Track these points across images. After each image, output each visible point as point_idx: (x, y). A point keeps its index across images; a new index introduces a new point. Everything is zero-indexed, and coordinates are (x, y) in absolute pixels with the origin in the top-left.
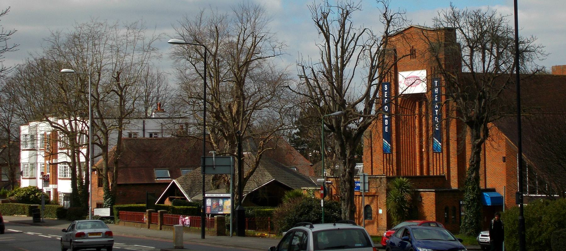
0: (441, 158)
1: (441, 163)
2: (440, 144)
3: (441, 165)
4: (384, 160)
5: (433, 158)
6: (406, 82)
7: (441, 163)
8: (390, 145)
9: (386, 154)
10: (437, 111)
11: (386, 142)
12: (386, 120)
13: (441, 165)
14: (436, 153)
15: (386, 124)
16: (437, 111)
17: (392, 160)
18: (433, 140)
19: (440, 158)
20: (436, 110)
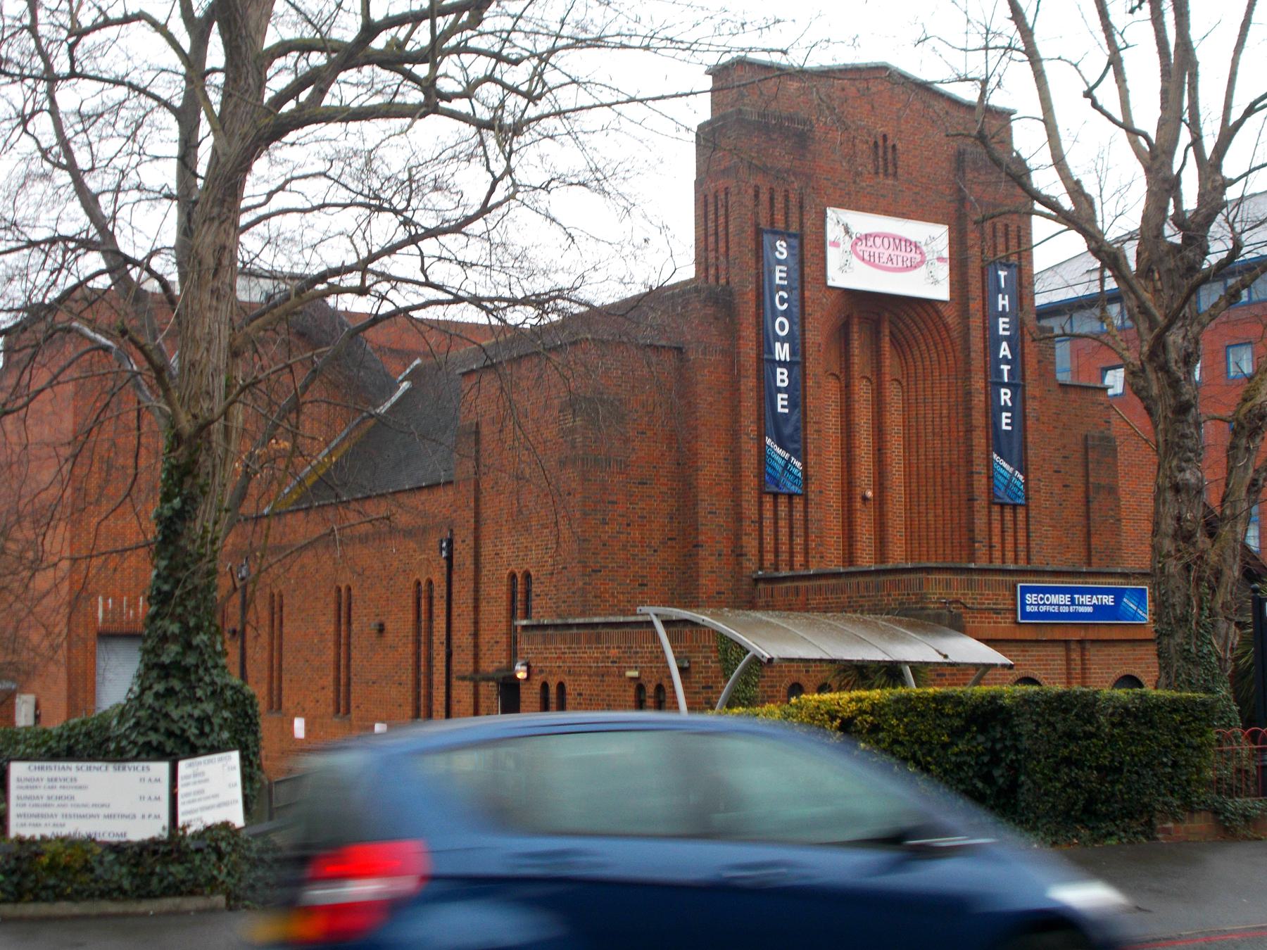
0: (1021, 524)
1: (1022, 538)
2: (1021, 477)
3: (1021, 547)
5: (990, 523)
6: (858, 248)
7: (1022, 538)
8: (798, 464)
9: (775, 496)
10: (1005, 368)
11: (779, 451)
12: (779, 370)
13: (1021, 547)
14: (1002, 506)
15: (779, 384)
16: (1005, 368)
17: (806, 520)
18: (990, 462)
19: (1015, 524)
20: (1002, 367)
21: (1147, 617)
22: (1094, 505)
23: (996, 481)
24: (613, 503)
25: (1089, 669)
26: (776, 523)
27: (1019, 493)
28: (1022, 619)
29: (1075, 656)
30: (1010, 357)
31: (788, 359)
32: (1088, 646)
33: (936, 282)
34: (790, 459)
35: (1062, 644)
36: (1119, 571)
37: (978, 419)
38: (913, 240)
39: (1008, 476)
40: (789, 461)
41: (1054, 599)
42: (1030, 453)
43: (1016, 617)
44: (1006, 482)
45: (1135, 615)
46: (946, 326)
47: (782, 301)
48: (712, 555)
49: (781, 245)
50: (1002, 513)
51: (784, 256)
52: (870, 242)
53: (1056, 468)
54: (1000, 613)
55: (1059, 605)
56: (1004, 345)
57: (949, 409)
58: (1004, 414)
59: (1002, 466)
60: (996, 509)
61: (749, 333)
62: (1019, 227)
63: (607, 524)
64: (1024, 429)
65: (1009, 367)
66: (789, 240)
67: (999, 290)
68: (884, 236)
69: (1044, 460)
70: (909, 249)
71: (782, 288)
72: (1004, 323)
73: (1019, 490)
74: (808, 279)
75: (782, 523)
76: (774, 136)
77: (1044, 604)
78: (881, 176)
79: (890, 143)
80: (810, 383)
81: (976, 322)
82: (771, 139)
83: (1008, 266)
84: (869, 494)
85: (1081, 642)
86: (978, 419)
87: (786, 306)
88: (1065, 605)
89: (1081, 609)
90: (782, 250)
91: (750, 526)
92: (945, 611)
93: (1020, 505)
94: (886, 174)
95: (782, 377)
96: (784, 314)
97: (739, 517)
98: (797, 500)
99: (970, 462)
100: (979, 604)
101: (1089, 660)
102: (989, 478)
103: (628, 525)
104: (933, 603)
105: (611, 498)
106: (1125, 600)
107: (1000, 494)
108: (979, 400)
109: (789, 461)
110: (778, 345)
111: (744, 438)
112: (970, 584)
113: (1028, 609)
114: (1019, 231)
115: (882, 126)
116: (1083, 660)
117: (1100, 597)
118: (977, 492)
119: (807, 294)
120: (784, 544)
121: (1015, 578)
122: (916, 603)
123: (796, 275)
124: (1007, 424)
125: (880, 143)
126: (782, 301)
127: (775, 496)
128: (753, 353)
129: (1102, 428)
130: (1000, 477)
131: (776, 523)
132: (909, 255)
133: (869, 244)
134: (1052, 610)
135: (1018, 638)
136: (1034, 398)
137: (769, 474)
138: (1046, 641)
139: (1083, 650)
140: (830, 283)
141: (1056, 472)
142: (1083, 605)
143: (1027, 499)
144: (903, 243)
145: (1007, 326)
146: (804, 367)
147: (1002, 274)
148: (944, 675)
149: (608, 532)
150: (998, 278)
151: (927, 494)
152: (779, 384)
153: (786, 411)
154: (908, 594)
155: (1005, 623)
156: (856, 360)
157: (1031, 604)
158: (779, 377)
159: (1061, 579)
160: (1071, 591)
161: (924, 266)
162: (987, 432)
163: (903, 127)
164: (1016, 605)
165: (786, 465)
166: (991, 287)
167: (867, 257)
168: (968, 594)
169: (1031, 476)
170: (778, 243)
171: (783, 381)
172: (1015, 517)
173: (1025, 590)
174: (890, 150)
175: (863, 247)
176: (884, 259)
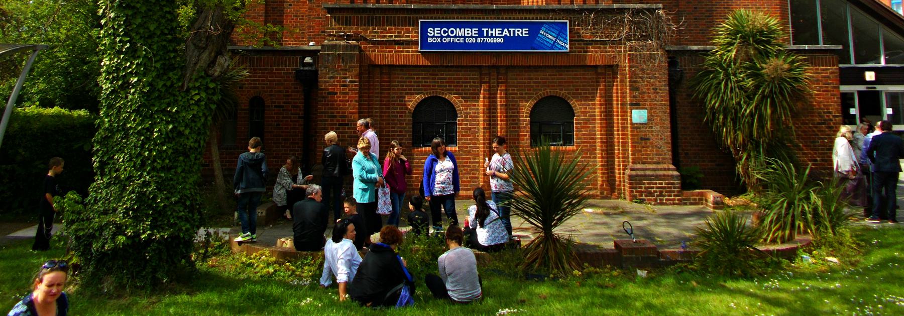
21: (568, 46)
41: (459, 32)
55: (465, 37)
77: (448, 36)
88: (472, 37)
89: (491, 40)
106: (541, 32)
113: (430, 40)
117: (512, 30)
134: (456, 40)
138: (451, 67)
142: (492, 36)
157: (432, 37)
160: (479, 26)
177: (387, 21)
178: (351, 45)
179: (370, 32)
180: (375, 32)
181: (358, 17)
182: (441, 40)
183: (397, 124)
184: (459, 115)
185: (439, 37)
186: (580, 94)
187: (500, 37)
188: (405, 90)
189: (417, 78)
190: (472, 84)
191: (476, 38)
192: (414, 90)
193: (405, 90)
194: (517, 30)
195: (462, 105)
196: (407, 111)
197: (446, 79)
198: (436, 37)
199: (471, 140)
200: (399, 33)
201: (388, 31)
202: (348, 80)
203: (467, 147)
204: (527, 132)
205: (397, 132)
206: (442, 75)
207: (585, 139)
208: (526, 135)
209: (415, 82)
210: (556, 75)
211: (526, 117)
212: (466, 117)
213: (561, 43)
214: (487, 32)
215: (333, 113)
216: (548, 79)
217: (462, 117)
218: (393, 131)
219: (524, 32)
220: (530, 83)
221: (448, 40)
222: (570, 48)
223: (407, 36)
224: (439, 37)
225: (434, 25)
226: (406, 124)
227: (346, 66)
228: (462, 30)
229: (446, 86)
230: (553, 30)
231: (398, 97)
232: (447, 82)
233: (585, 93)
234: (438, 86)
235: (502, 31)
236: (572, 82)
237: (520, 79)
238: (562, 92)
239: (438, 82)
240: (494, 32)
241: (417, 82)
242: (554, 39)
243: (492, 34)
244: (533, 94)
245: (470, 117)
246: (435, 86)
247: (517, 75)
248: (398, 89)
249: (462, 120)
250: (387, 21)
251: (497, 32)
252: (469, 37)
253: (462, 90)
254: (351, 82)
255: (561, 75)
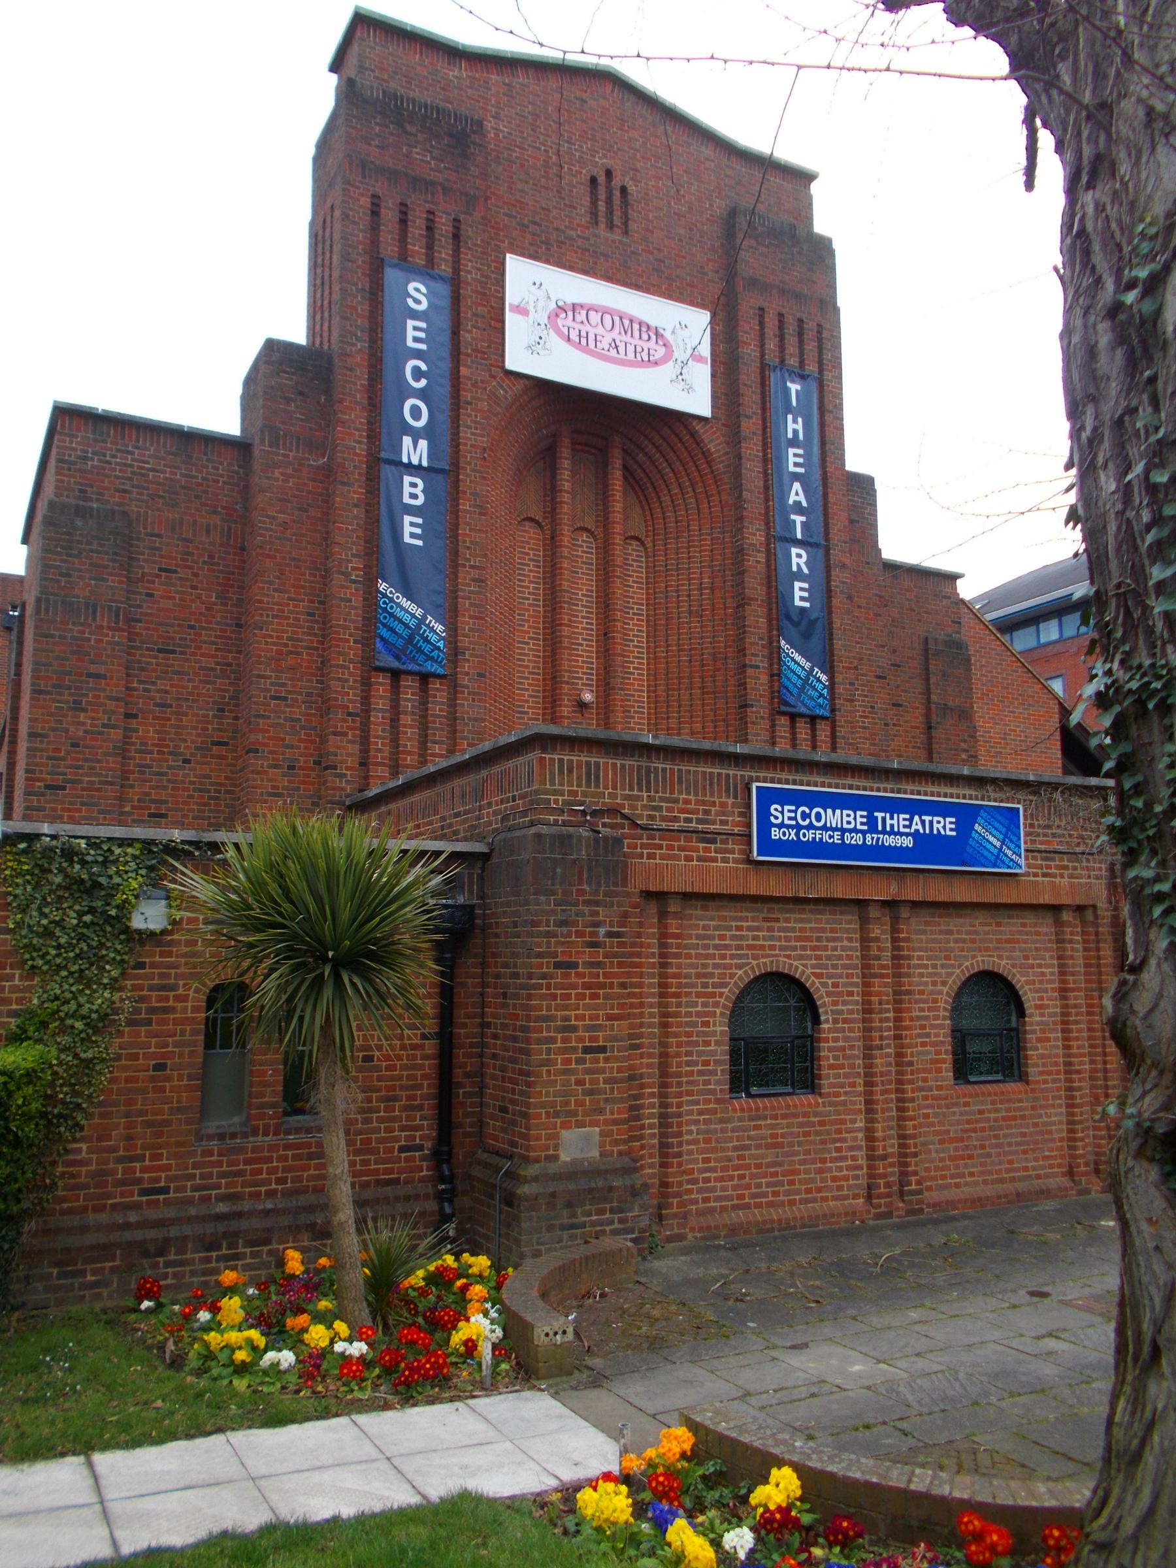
2: (824, 678)
4: (366, 699)
6: (560, 322)
10: (799, 519)
12: (407, 479)
14: (793, 717)
15: (407, 500)
16: (799, 519)
17: (453, 718)
20: (793, 517)
21: (1022, 862)
22: (938, 734)
23: (784, 680)
24: (98, 676)
25: (909, 958)
26: (395, 722)
27: (821, 700)
28: (759, 854)
29: (880, 931)
30: (805, 504)
31: (425, 463)
32: (904, 912)
33: (690, 389)
34: (424, 617)
35: (855, 909)
36: (966, 771)
37: (755, 587)
38: (653, 323)
39: (803, 675)
40: (422, 621)
41: (833, 817)
42: (838, 644)
43: (751, 851)
44: (799, 683)
45: (997, 857)
46: (706, 455)
47: (418, 374)
48: (275, 766)
49: (417, 290)
50: (793, 727)
51: (424, 306)
52: (581, 316)
53: (879, 672)
54: (714, 841)
55: (843, 831)
56: (797, 486)
57: (712, 577)
58: (797, 585)
59: (793, 659)
60: (783, 721)
61: (354, 417)
62: (819, 325)
63: (83, 710)
64: (829, 609)
65: (804, 519)
66: (432, 284)
67: (788, 409)
68: (604, 311)
69: (861, 659)
70: (645, 336)
71: (418, 354)
72: (795, 455)
73: (821, 695)
74: (466, 349)
75: (406, 720)
76: (408, 128)
77: (811, 827)
78: (602, 226)
79: (617, 182)
80: (464, 505)
81: (752, 449)
82: (406, 132)
83: (803, 377)
84: (588, 697)
85: (890, 905)
86: (755, 587)
87: (423, 383)
88: (855, 830)
89: (890, 841)
90: (418, 294)
91: (344, 720)
92: (584, 832)
93: (823, 718)
94: (611, 226)
95: (413, 490)
96: (422, 394)
97: (324, 705)
98: (435, 685)
99: (742, 651)
100: (664, 819)
101: (907, 940)
102: (772, 676)
103: (127, 716)
104: (553, 811)
105: (93, 669)
106: (977, 827)
107: (791, 700)
108: (756, 561)
109: (422, 621)
110: (407, 441)
111: (337, 579)
112: (645, 780)
113: (775, 834)
114: (819, 332)
115: (605, 156)
116: (894, 940)
117: (927, 818)
118: (752, 696)
119: (464, 371)
120: (410, 753)
121: (748, 773)
122: (524, 813)
123: (445, 338)
124: (802, 599)
125: (602, 179)
126: (418, 374)
127: (396, 674)
128: (361, 449)
129: (950, 630)
130: (791, 675)
131: (395, 722)
132: (646, 345)
133: (579, 318)
134: (826, 838)
135: (753, 892)
136: (844, 566)
137: (383, 639)
139: (895, 920)
140: (510, 364)
141: (879, 677)
142: (892, 832)
143: (833, 711)
144: (636, 327)
145: (800, 460)
146: (456, 482)
147: (794, 387)
148: (575, 965)
149: (84, 724)
150: (787, 391)
151: (679, 700)
152: (407, 500)
153: (420, 543)
154: (514, 799)
155: (725, 860)
156: (566, 497)
158: (407, 490)
159: (849, 781)
160: (870, 805)
161: (671, 363)
162: (770, 610)
163: (639, 165)
164: (749, 825)
165: (418, 627)
166: (776, 402)
167: (574, 336)
168: (639, 798)
169: (839, 678)
170: (411, 287)
171: (414, 496)
172: (814, 736)
173: (768, 797)
174: (617, 194)
175: (569, 322)
176: (605, 343)
177: (680, 782)
178: (605, 838)
179: (644, 807)
180: (655, 808)
181: (614, 765)
182: (797, 834)
183: (696, 1044)
184: (823, 1018)
185: (792, 827)
186: (1032, 967)
187: (907, 835)
188: (713, 957)
189: (739, 928)
190: (846, 943)
191: (864, 833)
192: (732, 957)
193: (713, 957)
194: (936, 819)
195: (828, 994)
196: (718, 1011)
197: (793, 930)
198: (788, 827)
199: (846, 1076)
200: (706, 812)
201: (681, 805)
202: (602, 931)
203: (837, 1095)
204: (946, 1052)
205: (695, 1063)
206: (787, 920)
207: (1044, 1065)
208: (944, 1061)
209: (733, 938)
210: (990, 924)
211: (944, 1018)
212: (835, 1021)
213: (1009, 853)
214: (884, 819)
215: (568, 1019)
216: (977, 933)
217: (827, 1021)
218: (688, 1064)
219: (948, 826)
220: (948, 941)
221: (810, 835)
222: (1029, 866)
223: (723, 823)
224: (792, 827)
225: (785, 798)
226: (717, 1043)
227: (596, 893)
228: (838, 812)
229: (794, 948)
230: (997, 825)
231: (698, 976)
232: (798, 939)
233: (1040, 966)
234: (782, 948)
235: (911, 820)
236: (1018, 941)
237: (932, 932)
238: (1003, 963)
239: (780, 938)
240: (895, 822)
241: (741, 938)
242: (998, 844)
243: (892, 826)
244: (953, 966)
245: (845, 1021)
246: (772, 947)
247: (927, 924)
248: (698, 956)
249: (830, 1030)
250: (680, 782)
251: (902, 823)
252: (850, 831)
253: (828, 958)
254: (610, 934)
255: (999, 924)
